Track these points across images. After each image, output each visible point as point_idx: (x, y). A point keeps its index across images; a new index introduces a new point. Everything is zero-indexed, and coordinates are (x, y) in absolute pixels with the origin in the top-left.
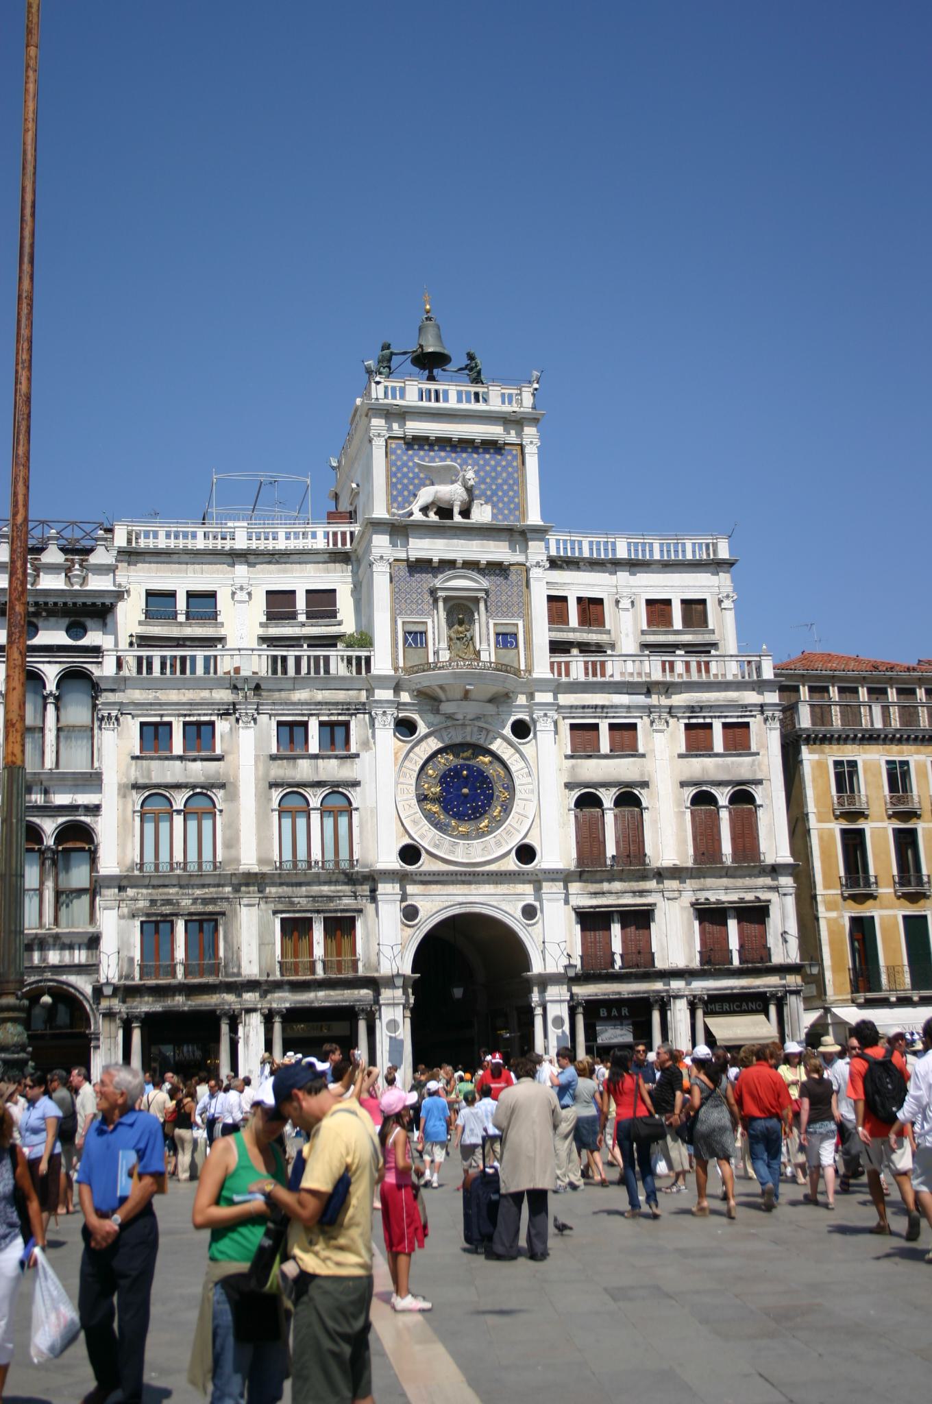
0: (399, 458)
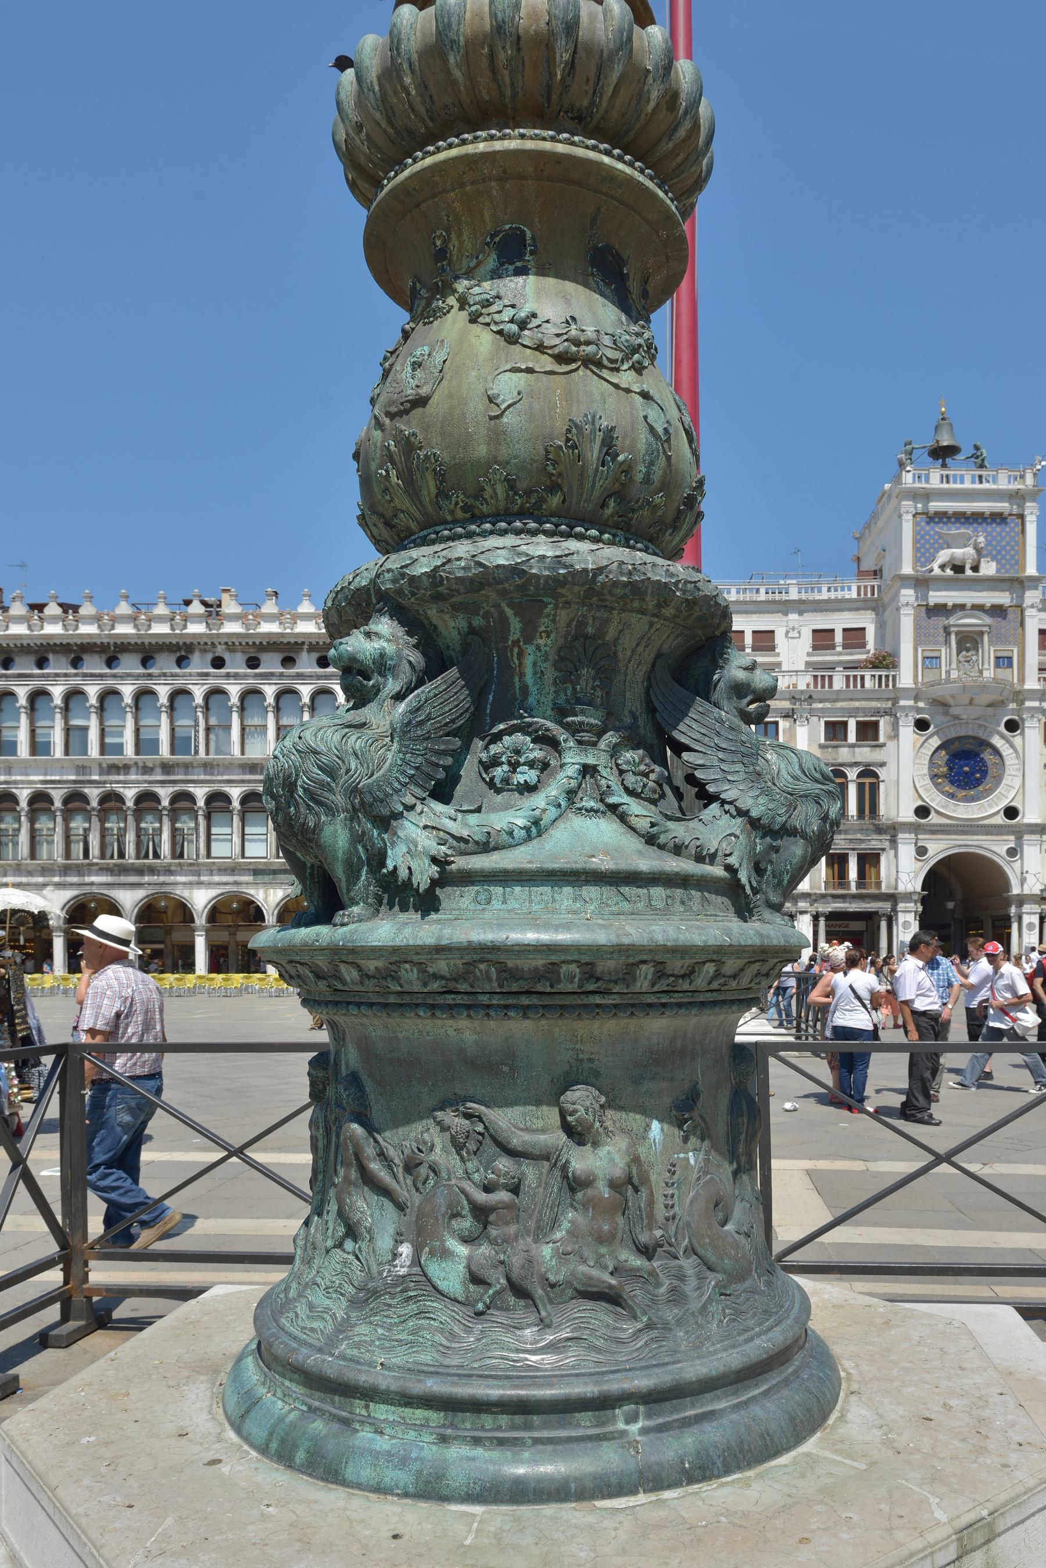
0: (922, 529)
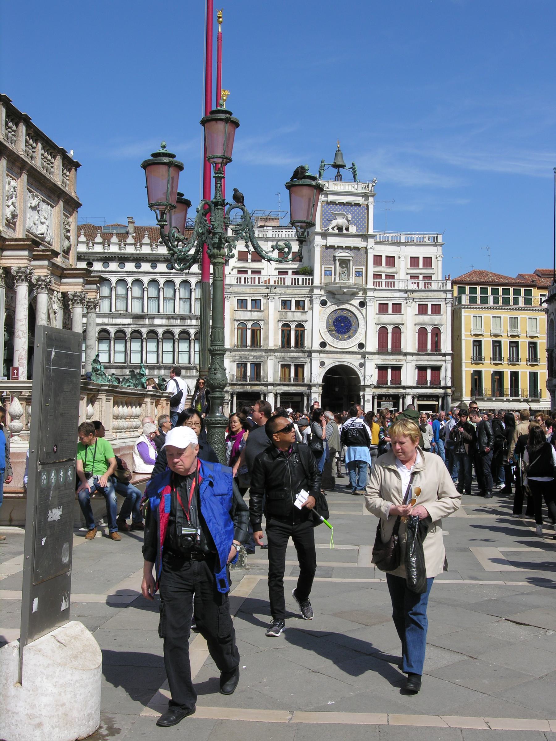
0: (325, 209)
